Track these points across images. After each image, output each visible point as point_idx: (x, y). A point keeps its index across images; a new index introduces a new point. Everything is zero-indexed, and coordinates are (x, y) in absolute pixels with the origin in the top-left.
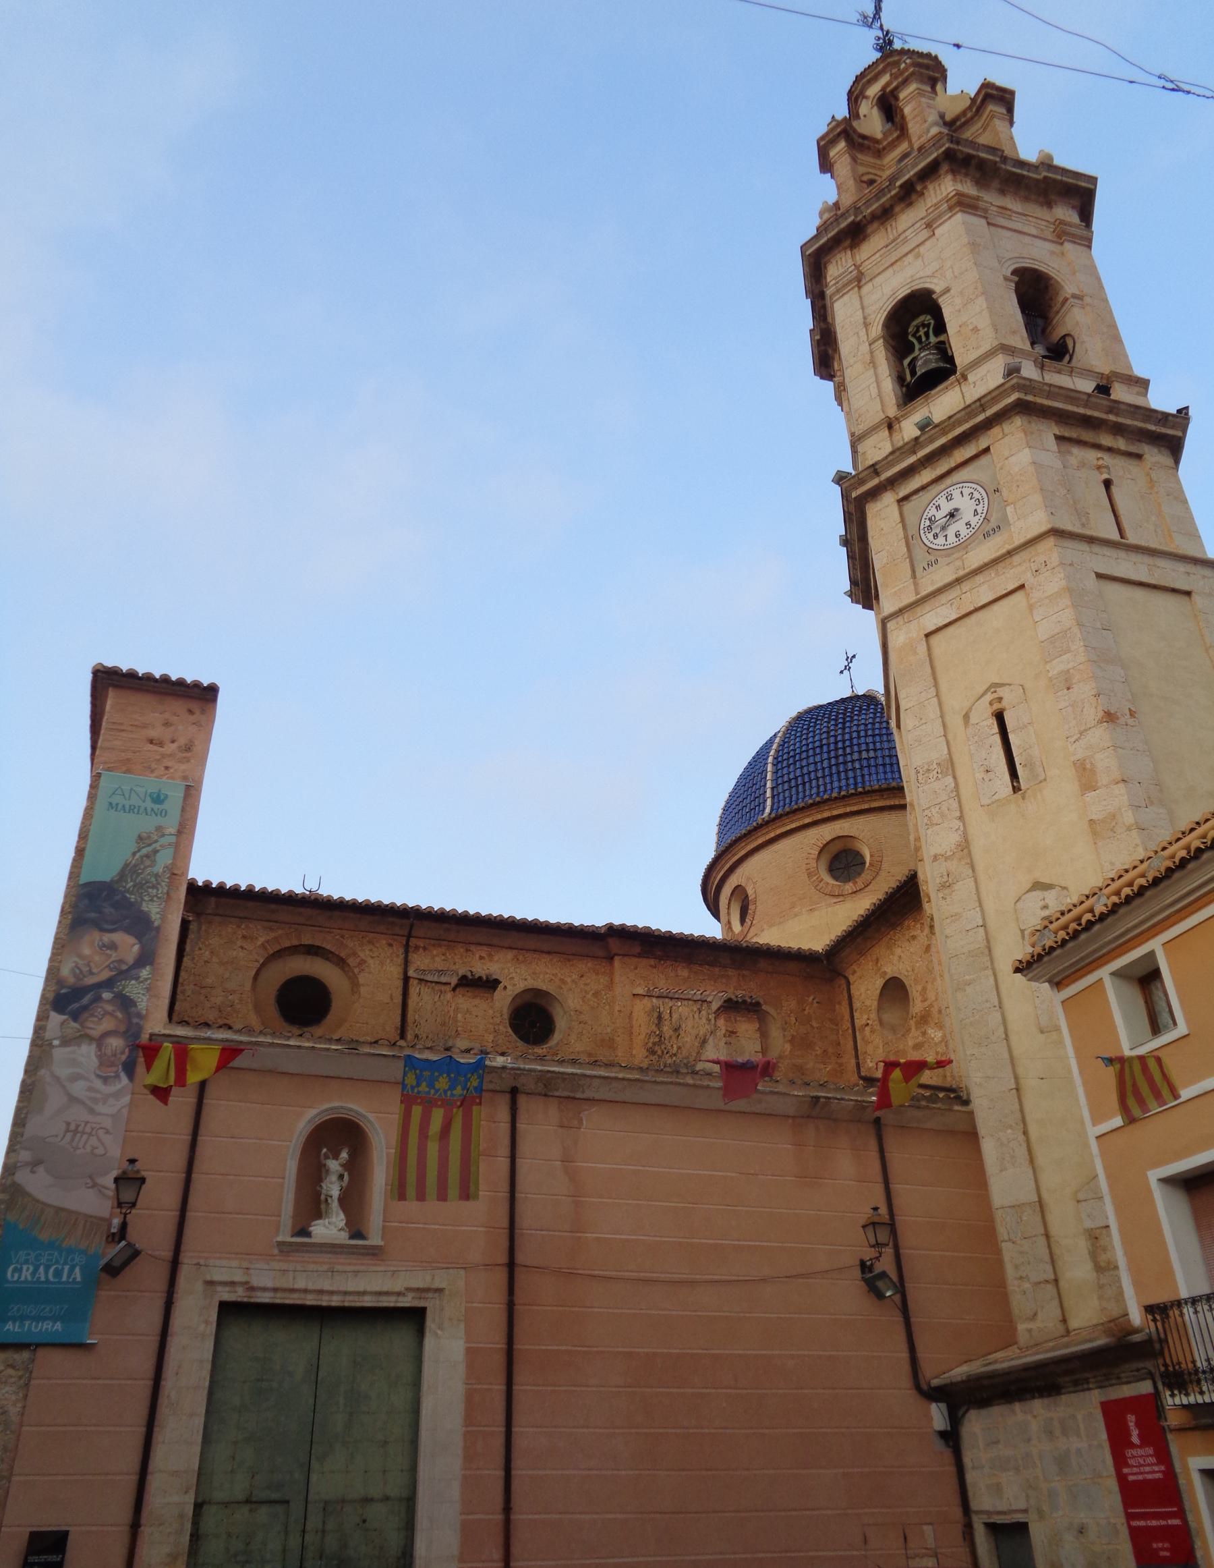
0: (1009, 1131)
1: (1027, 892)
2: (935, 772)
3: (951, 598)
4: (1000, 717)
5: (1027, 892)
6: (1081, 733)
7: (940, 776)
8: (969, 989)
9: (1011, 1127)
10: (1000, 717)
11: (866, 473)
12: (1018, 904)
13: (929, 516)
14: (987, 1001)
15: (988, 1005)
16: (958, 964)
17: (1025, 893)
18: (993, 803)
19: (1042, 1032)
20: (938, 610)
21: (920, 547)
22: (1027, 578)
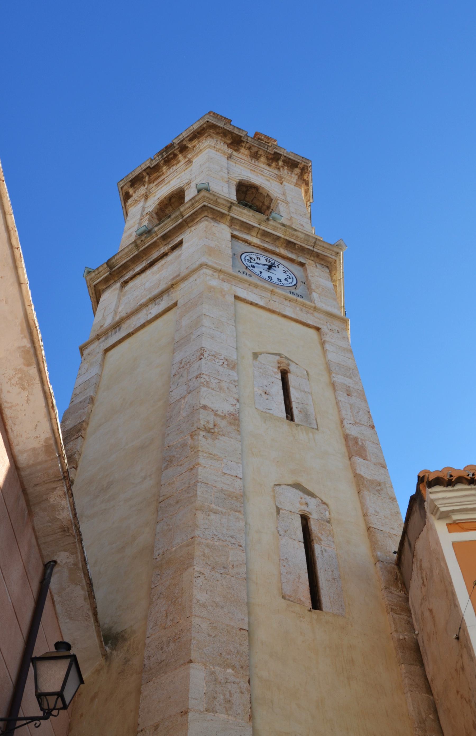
0: (230, 671)
1: (288, 485)
2: (221, 361)
3: (262, 295)
4: (284, 375)
5: (288, 485)
6: (356, 423)
7: (225, 366)
8: (213, 516)
9: (233, 667)
10: (284, 375)
11: (224, 202)
12: (277, 487)
13: (252, 256)
14: (232, 537)
15: (233, 541)
16: (207, 491)
17: (285, 484)
18: (266, 412)
19: (284, 597)
20: (250, 293)
21: (239, 262)
22: (324, 329)
